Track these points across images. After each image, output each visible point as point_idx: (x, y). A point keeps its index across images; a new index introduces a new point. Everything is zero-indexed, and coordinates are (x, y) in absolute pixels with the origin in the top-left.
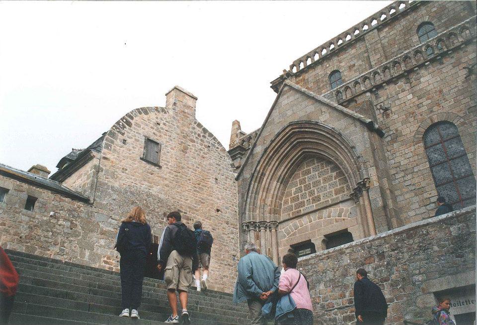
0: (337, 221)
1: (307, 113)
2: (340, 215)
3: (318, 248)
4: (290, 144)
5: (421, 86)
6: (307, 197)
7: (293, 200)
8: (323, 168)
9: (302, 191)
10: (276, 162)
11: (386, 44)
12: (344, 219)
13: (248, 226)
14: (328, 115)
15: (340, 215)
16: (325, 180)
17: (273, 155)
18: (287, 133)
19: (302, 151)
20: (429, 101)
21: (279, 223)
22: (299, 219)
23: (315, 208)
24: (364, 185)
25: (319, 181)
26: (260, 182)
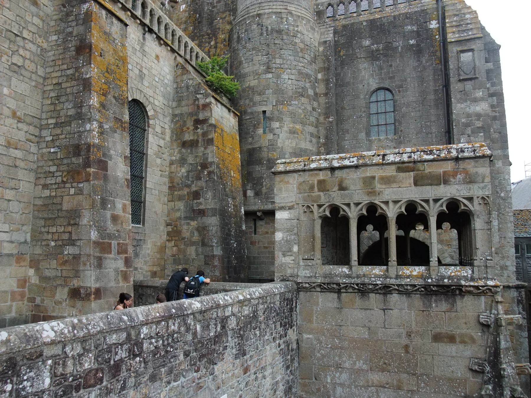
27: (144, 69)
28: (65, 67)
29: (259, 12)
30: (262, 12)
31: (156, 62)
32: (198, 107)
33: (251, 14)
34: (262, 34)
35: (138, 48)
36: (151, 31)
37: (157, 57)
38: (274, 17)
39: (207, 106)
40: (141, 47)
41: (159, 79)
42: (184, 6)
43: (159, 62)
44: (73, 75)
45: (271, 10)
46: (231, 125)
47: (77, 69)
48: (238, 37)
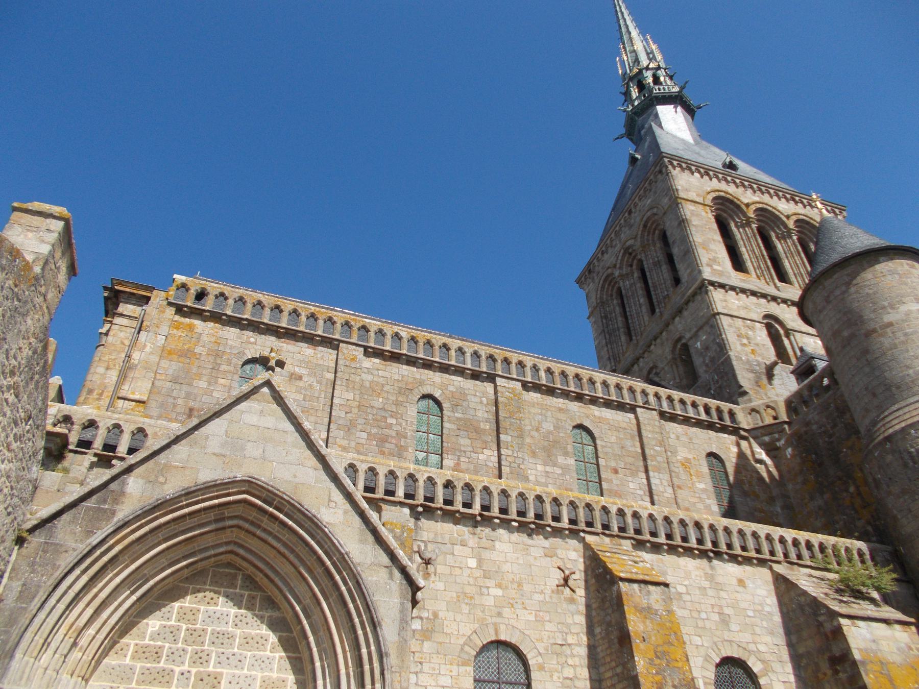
1: (297, 480)
5: (494, 556)
7: (142, 653)
11: (368, 385)
16: (247, 641)
19: (230, 548)
20: (499, 592)
25: (232, 637)
27: (725, 608)
28: (613, 664)
29: (886, 434)
30: (891, 431)
31: (741, 589)
32: (826, 635)
33: (876, 441)
34: (905, 465)
35: (706, 584)
36: (718, 555)
37: (741, 582)
38: (913, 432)
39: (838, 632)
40: (711, 582)
41: (754, 611)
42: (790, 450)
43: (745, 587)
44: (623, 673)
45: (903, 424)
46: (903, 645)
47: (624, 665)
48: (874, 479)
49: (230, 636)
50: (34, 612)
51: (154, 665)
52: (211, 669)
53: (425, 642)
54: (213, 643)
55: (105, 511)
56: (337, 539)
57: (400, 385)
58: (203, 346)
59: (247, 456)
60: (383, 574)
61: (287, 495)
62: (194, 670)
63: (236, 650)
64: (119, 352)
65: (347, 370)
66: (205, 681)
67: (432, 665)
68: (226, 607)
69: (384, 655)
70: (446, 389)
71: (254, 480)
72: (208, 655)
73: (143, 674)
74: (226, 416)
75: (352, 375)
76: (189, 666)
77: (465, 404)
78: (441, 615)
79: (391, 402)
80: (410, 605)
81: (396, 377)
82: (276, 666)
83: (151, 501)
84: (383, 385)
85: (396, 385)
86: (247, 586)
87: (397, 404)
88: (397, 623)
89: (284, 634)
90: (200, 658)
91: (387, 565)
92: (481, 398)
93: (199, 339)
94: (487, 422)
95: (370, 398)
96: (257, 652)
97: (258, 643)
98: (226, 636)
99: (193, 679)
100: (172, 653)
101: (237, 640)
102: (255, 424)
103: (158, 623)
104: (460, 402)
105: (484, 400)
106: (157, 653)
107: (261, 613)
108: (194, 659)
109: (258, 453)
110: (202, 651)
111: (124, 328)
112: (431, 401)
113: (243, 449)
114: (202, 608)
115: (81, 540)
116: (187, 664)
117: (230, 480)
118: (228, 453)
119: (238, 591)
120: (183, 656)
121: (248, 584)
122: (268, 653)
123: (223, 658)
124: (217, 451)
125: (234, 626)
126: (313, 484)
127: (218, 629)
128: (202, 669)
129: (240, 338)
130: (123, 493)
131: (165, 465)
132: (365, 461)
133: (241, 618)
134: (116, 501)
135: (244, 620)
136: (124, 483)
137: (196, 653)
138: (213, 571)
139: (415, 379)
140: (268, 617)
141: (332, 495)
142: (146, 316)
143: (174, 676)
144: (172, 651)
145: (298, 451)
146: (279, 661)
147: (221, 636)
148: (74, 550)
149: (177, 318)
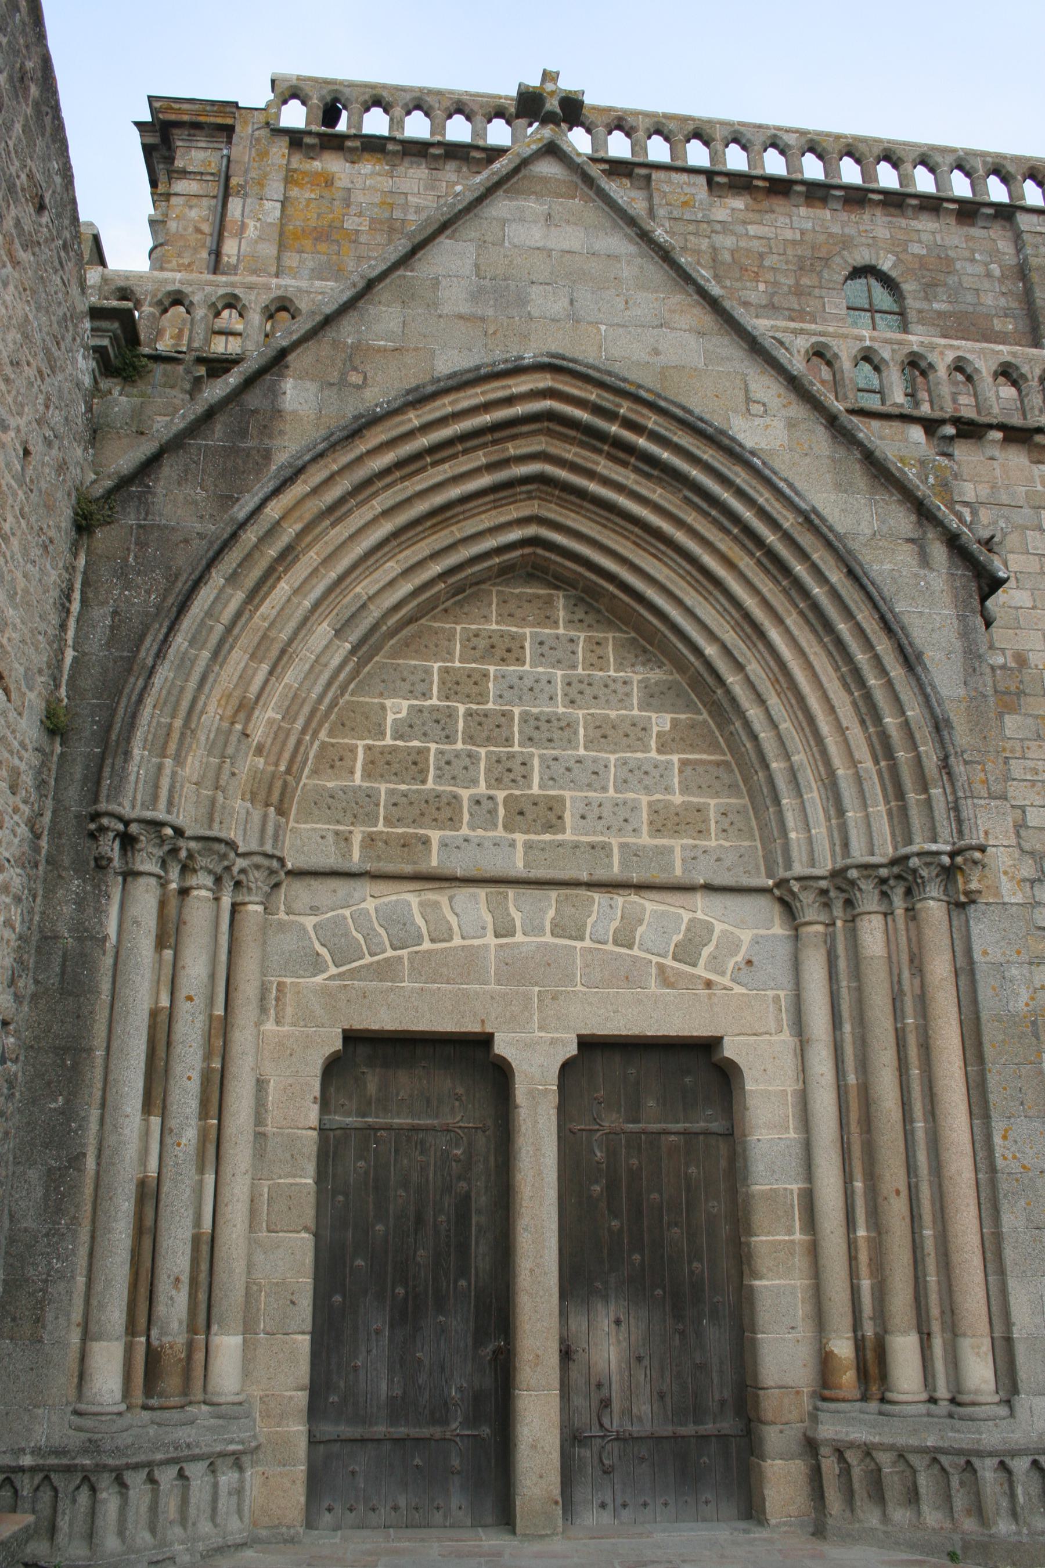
0: (665, 978)
2: (687, 952)
3: (531, 1093)
4: (490, 467)
6: (475, 782)
8: (598, 662)
9: (449, 738)
10: (375, 520)
11: (727, 257)
12: (709, 984)
13: (128, 841)
14: (778, 426)
15: (687, 952)
17: (387, 471)
18: (510, 401)
19: (531, 531)
21: (289, 873)
22: (431, 896)
23: (518, 865)
24: (949, 873)
25: (569, 726)
26: (255, 595)
49: (563, 724)
50: (150, 662)
51: (415, 787)
52: (535, 790)
53: (1007, 716)
54: (530, 739)
55: (248, 453)
56: (785, 480)
57: (799, 252)
58: (360, 215)
59: (535, 313)
60: (905, 557)
61: (648, 390)
62: (500, 795)
63: (582, 751)
64: (195, 250)
65: (679, 227)
66: (530, 816)
67: (1030, 764)
68: (541, 665)
69: (942, 725)
70: (905, 250)
71: (565, 363)
72: (524, 764)
73: (395, 805)
74: (470, 230)
75: (691, 238)
76: (488, 787)
77: (951, 280)
78: (1033, 658)
79: (786, 288)
80: (979, 621)
81: (789, 235)
82: (676, 780)
83: (342, 422)
84: (761, 256)
85: (790, 252)
86: (581, 621)
87: (799, 292)
88: (958, 658)
89: (683, 716)
90: (509, 770)
91: (911, 535)
92: (986, 265)
93: (347, 203)
94: (1006, 316)
95: (738, 285)
96: (629, 755)
97: (627, 735)
98: (555, 723)
99: (501, 811)
100: (448, 763)
101: (581, 731)
102: (540, 244)
103: (405, 704)
104: (941, 277)
105: (995, 268)
106: (415, 763)
107: (622, 674)
108: (496, 775)
109: (558, 306)
110: (511, 756)
111: (195, 201)
112: (873, 281)
113: (522, 301)
114: (492, 669)
115: (212, 516)
116: (482, 783)
117: (509, 366)
118: (490, 312)
119: (561, 631)
120: (471, 768)
121: (580, 614)
122: (653, 754)
123: (558, 769)
124: (464, 309)
125: (567, 703)
126: (701, 365)
127: (535, 710)
128: (517, 792)
129: (433, 188)
130: (277, 413)
131: (357, 347)
132: (802, 332)
133: (582, 686)
134: (266, 430)
135: (588, 691)
136: (275, 393)
137: (498, 761)
138: (498, 592)
139: (830, 235)
140: (639, 682)
141: (753, 386)
142: (232, 166)
143: (461, 807)
144: (446, 757)
145: (652, 296)
146: (681, 772)
147: (544, 726)
148: (201, 536)
149: (297, 161)
